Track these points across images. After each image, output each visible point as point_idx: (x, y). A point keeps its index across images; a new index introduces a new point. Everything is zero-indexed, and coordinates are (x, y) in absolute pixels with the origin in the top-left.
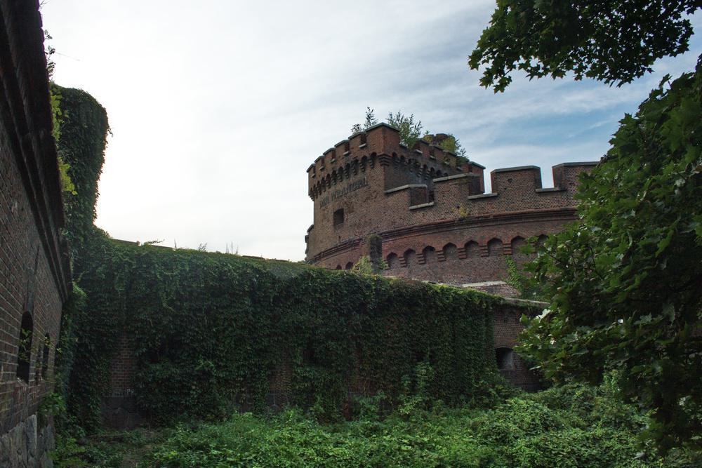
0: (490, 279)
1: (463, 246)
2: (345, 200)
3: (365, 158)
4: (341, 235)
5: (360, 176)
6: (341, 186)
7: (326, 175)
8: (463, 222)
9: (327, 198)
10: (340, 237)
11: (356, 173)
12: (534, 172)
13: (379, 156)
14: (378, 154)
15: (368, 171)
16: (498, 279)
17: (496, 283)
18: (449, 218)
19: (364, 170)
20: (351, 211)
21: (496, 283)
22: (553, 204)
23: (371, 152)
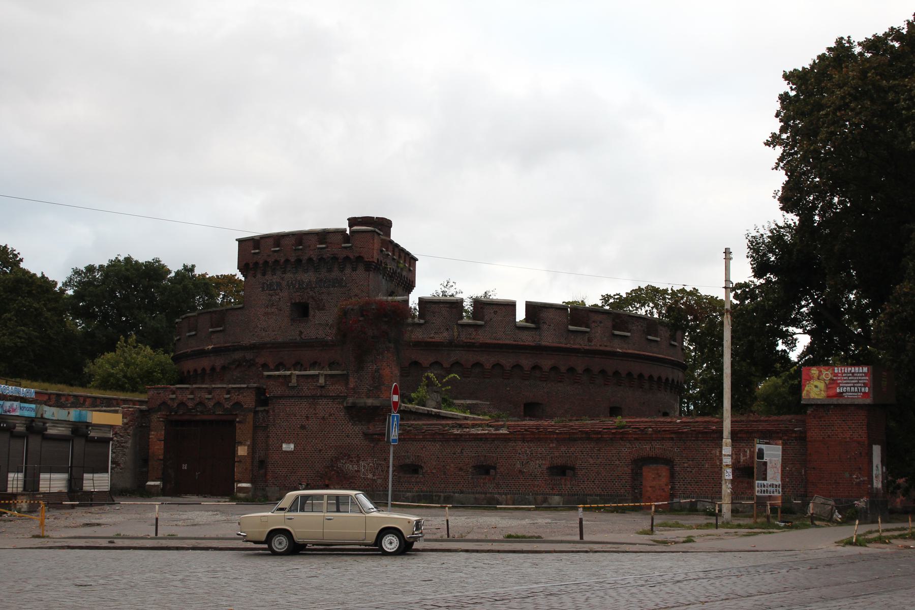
0: (469, 398)
1: (449, 366)
2: (311, 293)
3: (347, 258)
4: (303, 330)
5: (335, 274)
6: (308, 277)
7: (283, 260)
8: (451, 345)
9: (279, 284)
10: (301, 333)
11: (330, 270)
12: (511, 306)
13: (366, 262)
14: (366, 260)
15: (348, 271)
16: (476, 398)
17: (474, 402)
18: (438, 338)
19: (342, 270)
20: (321, 308)
21: (474, 402)
22: (527, 339)
23: (357, 255)
